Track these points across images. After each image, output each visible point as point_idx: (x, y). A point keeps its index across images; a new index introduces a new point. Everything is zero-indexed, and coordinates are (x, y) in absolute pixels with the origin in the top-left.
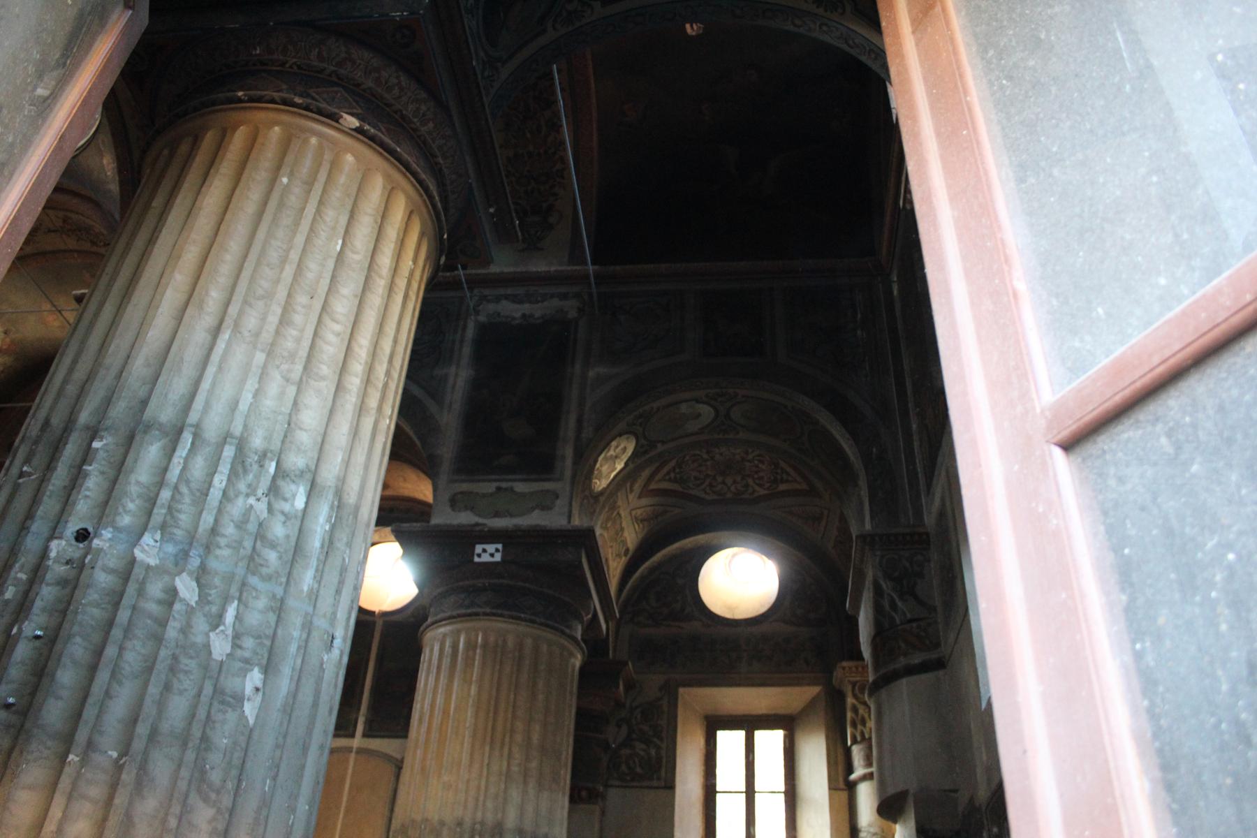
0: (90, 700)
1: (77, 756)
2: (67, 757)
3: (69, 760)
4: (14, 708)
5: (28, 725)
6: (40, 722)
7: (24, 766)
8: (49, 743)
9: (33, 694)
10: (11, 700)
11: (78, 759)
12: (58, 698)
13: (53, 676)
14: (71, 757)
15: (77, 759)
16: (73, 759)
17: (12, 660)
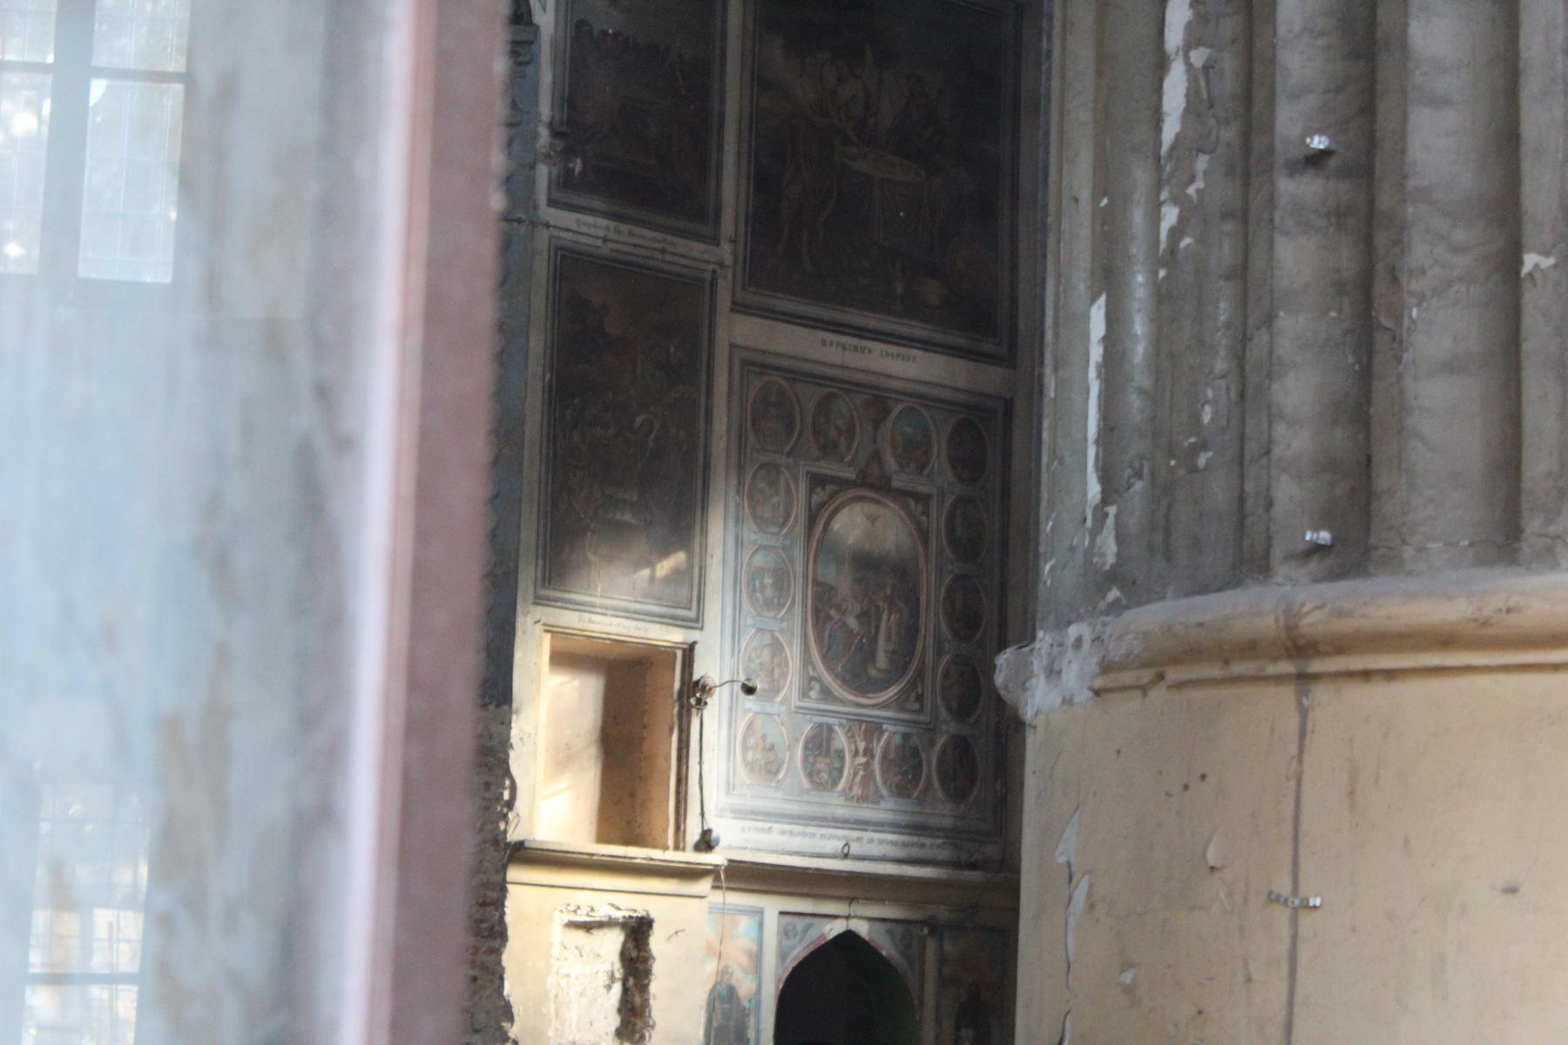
0: (1531, 86)
1: (1547, 254)
2: (1519, 262)
3: (1526, 269)
4: (1333, 162)
5: (1385, 201)
6: (1412, 184)
7: (1415, 312)
8: (1460, 235)
9: (1368, 110)
10: (1319, 142)
11: (1551, 261)
12: (1440, 103)
13: (1404, 45)
14: (1530, 260)
15: (1549, 262)
16: (1536, 266)
17: (1282, 30)
